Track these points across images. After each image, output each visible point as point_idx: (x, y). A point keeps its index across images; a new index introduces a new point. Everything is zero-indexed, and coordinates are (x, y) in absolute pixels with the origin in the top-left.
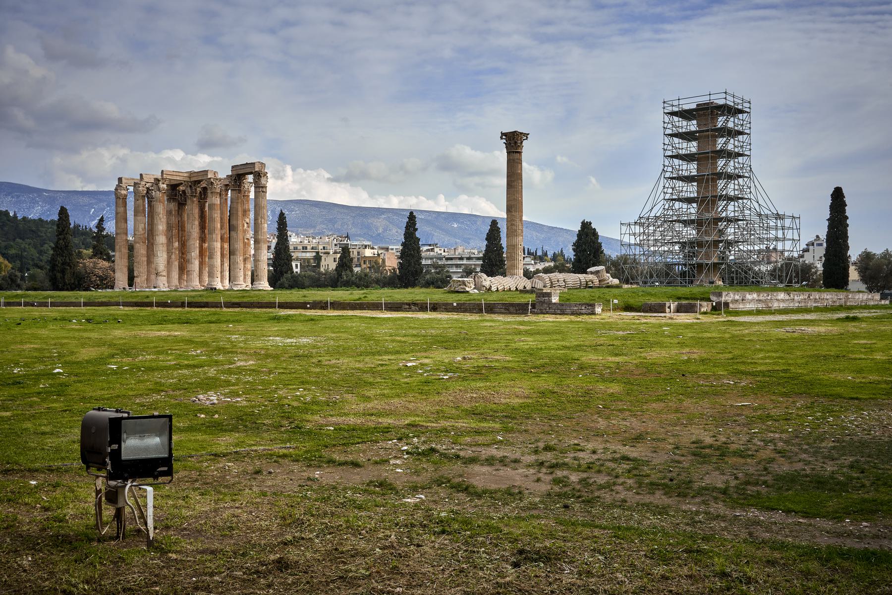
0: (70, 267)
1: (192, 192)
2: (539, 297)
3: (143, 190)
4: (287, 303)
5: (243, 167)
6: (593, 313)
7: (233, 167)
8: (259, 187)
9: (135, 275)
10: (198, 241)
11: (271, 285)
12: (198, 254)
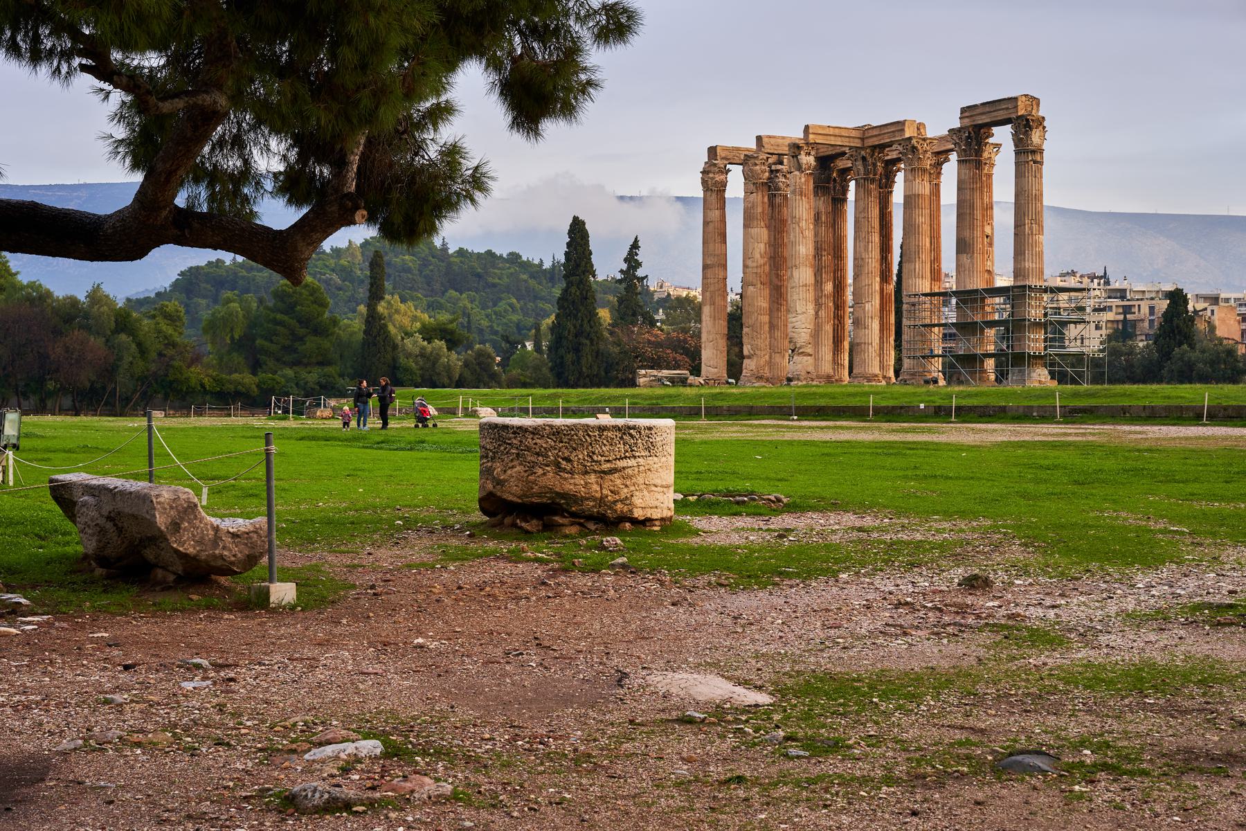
0: (592, 340)
1: (867, 172)
3: (763, 172)
4: (1226, 408)
5: (988, 109)
7: (963, 110)
9: (746, 352)
10: (878, 279)
12: (878, 306)
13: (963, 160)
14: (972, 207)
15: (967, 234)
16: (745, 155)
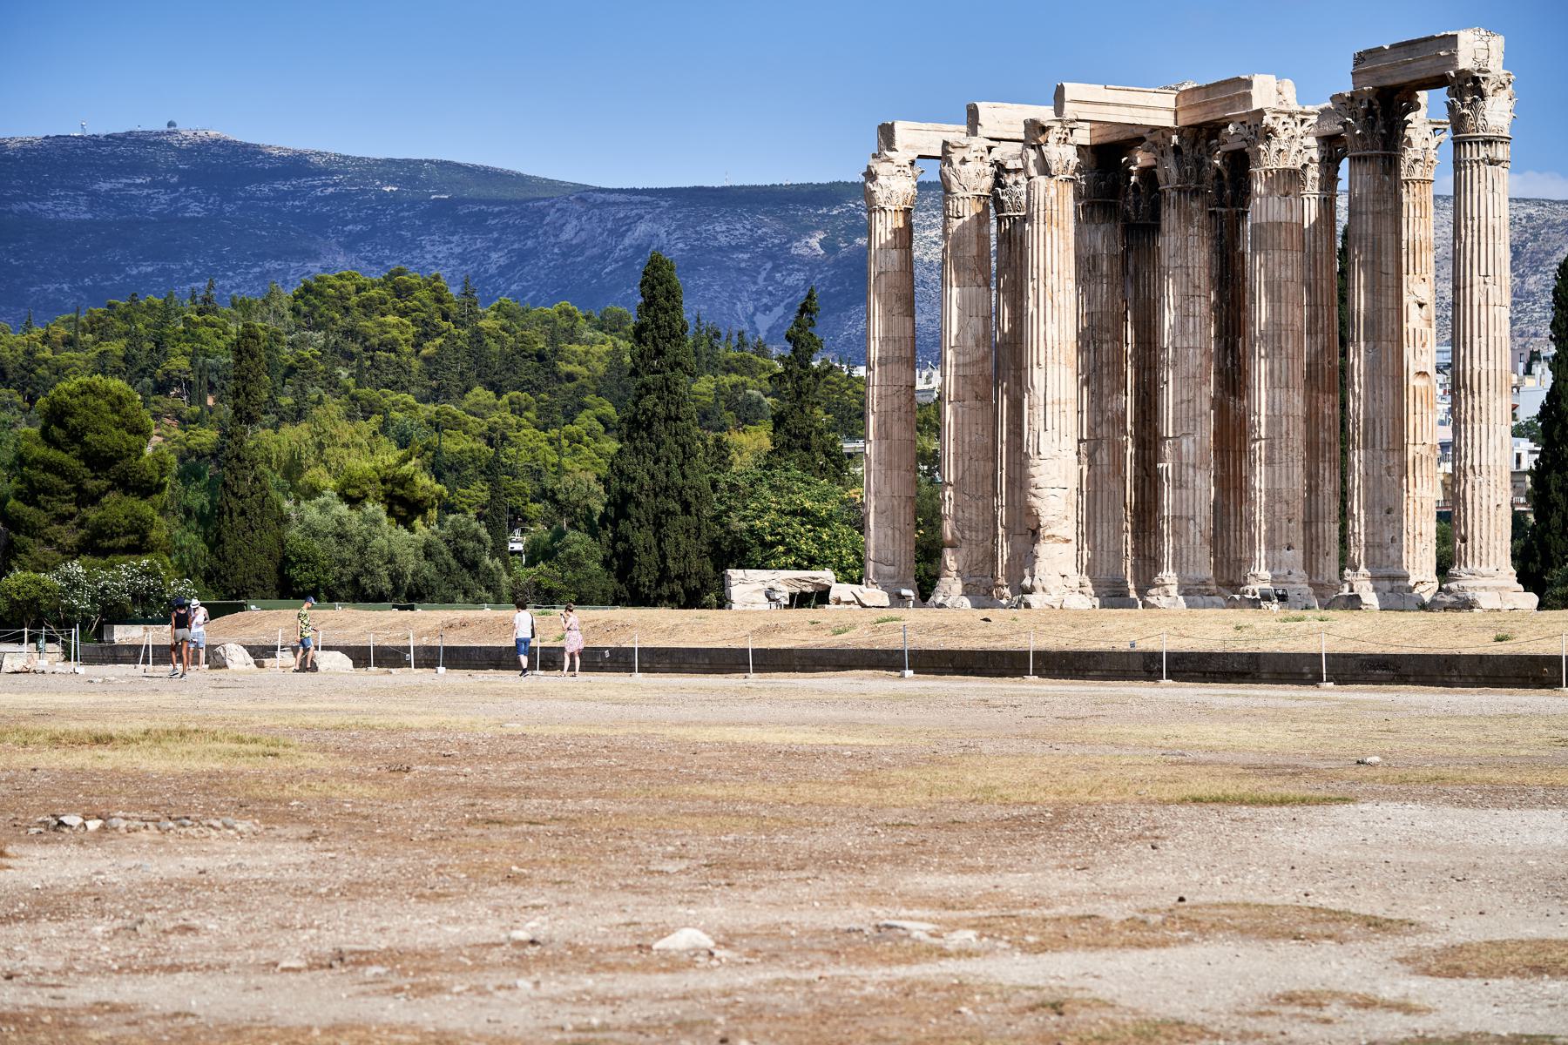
1: (1184, 176)
7: (1360, 59)
11: (1528, 579)
13: (1359, 158)
16: (945, 143)
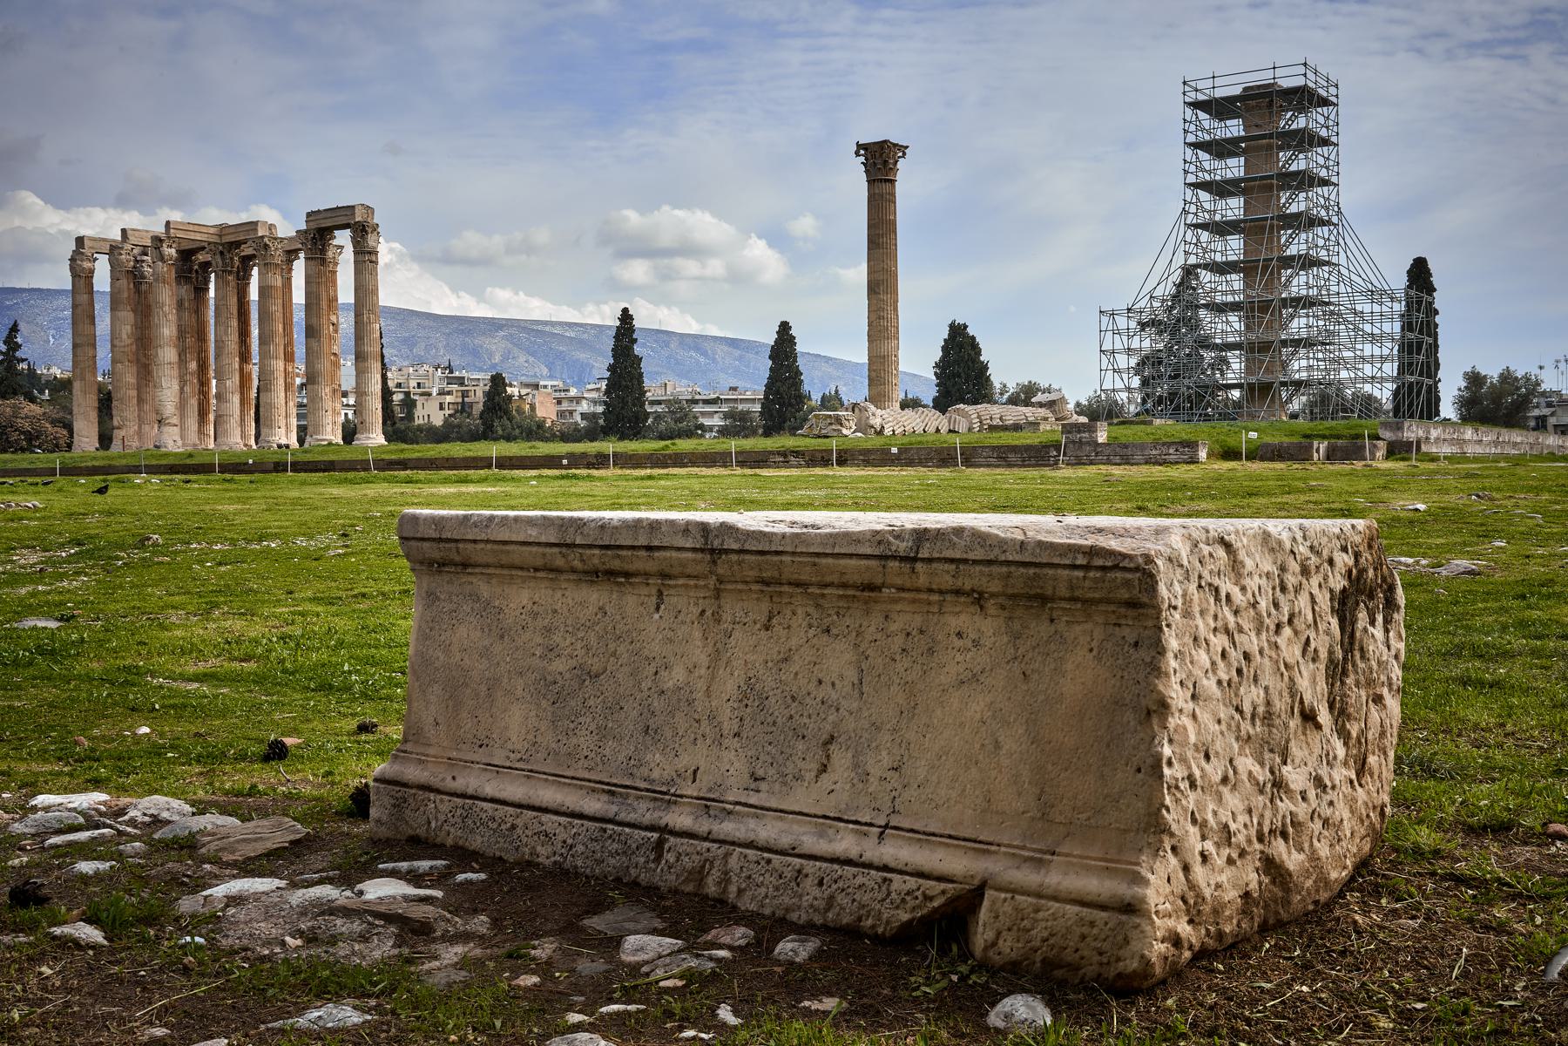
1: (225, 265)
2: (1070, 432)
6: (1193, 461)
7: (309, 215)
8: (364, 253)
14: (318, 298)
15: (314, 321)
